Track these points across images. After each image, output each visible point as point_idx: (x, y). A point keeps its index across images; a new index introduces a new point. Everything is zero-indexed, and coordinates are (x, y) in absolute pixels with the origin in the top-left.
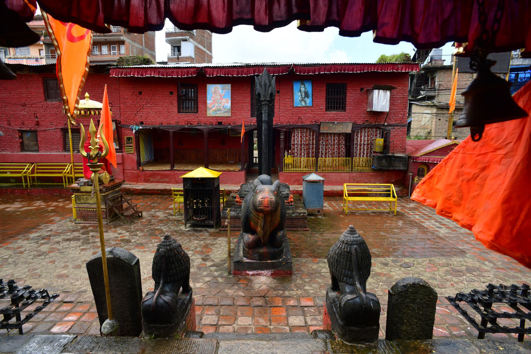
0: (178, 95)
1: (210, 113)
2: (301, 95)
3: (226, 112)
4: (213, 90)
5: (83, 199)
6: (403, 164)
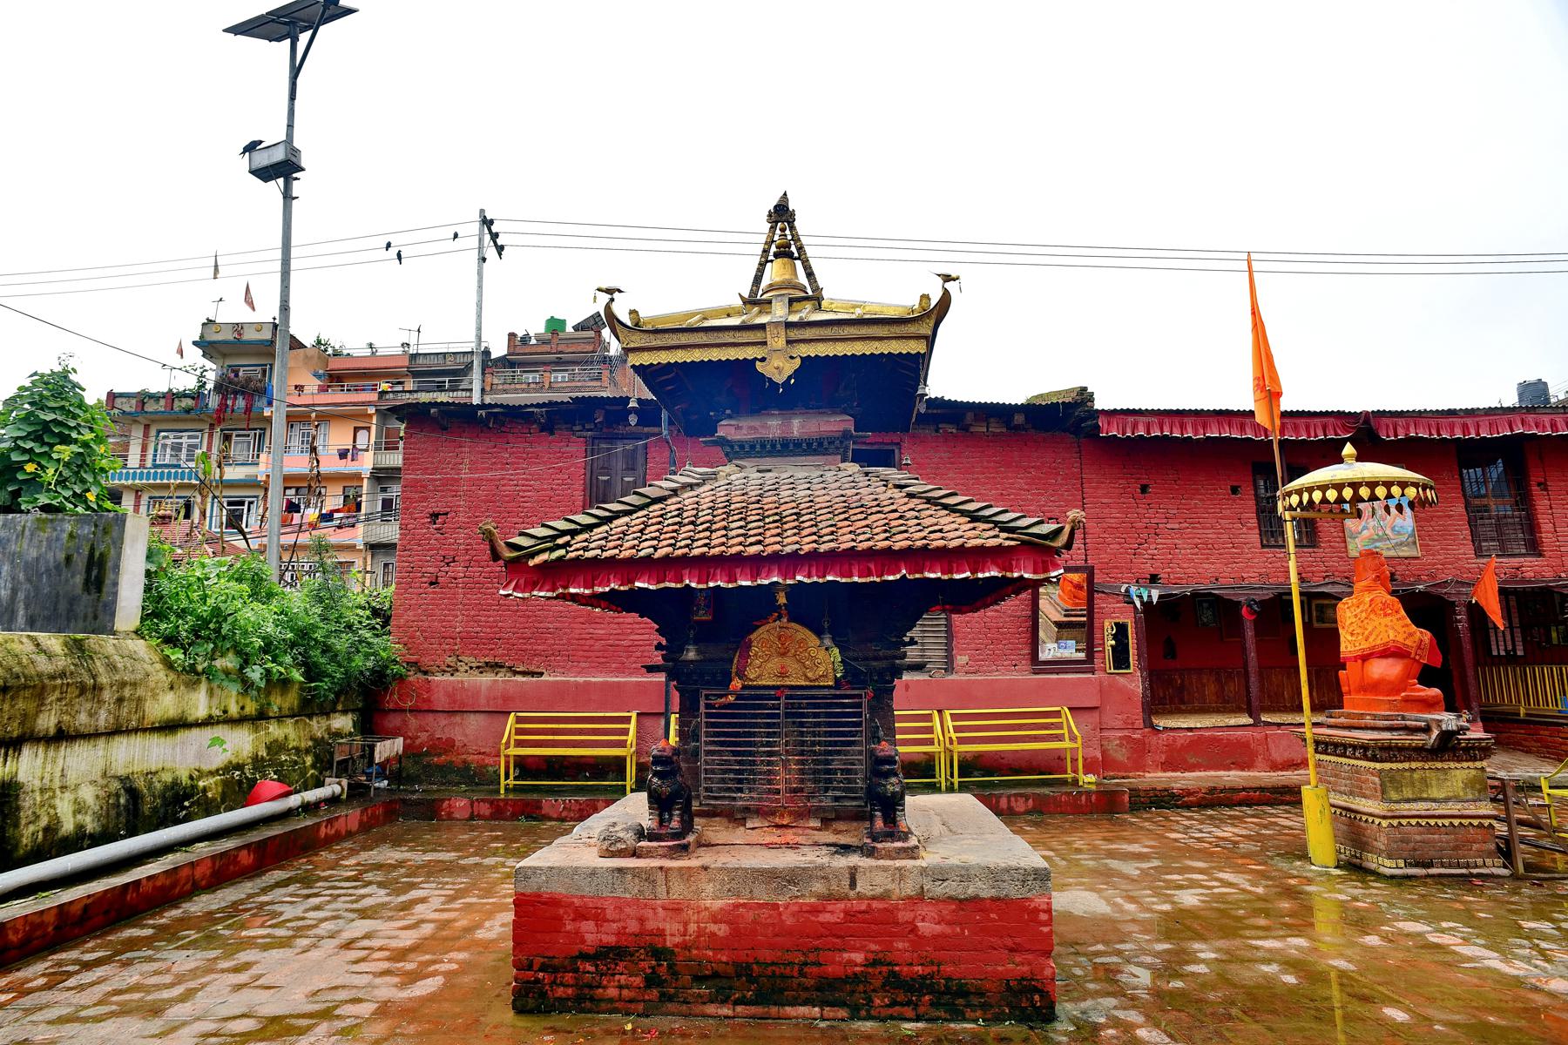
3: (1401, 544)
5: (1413, 784)
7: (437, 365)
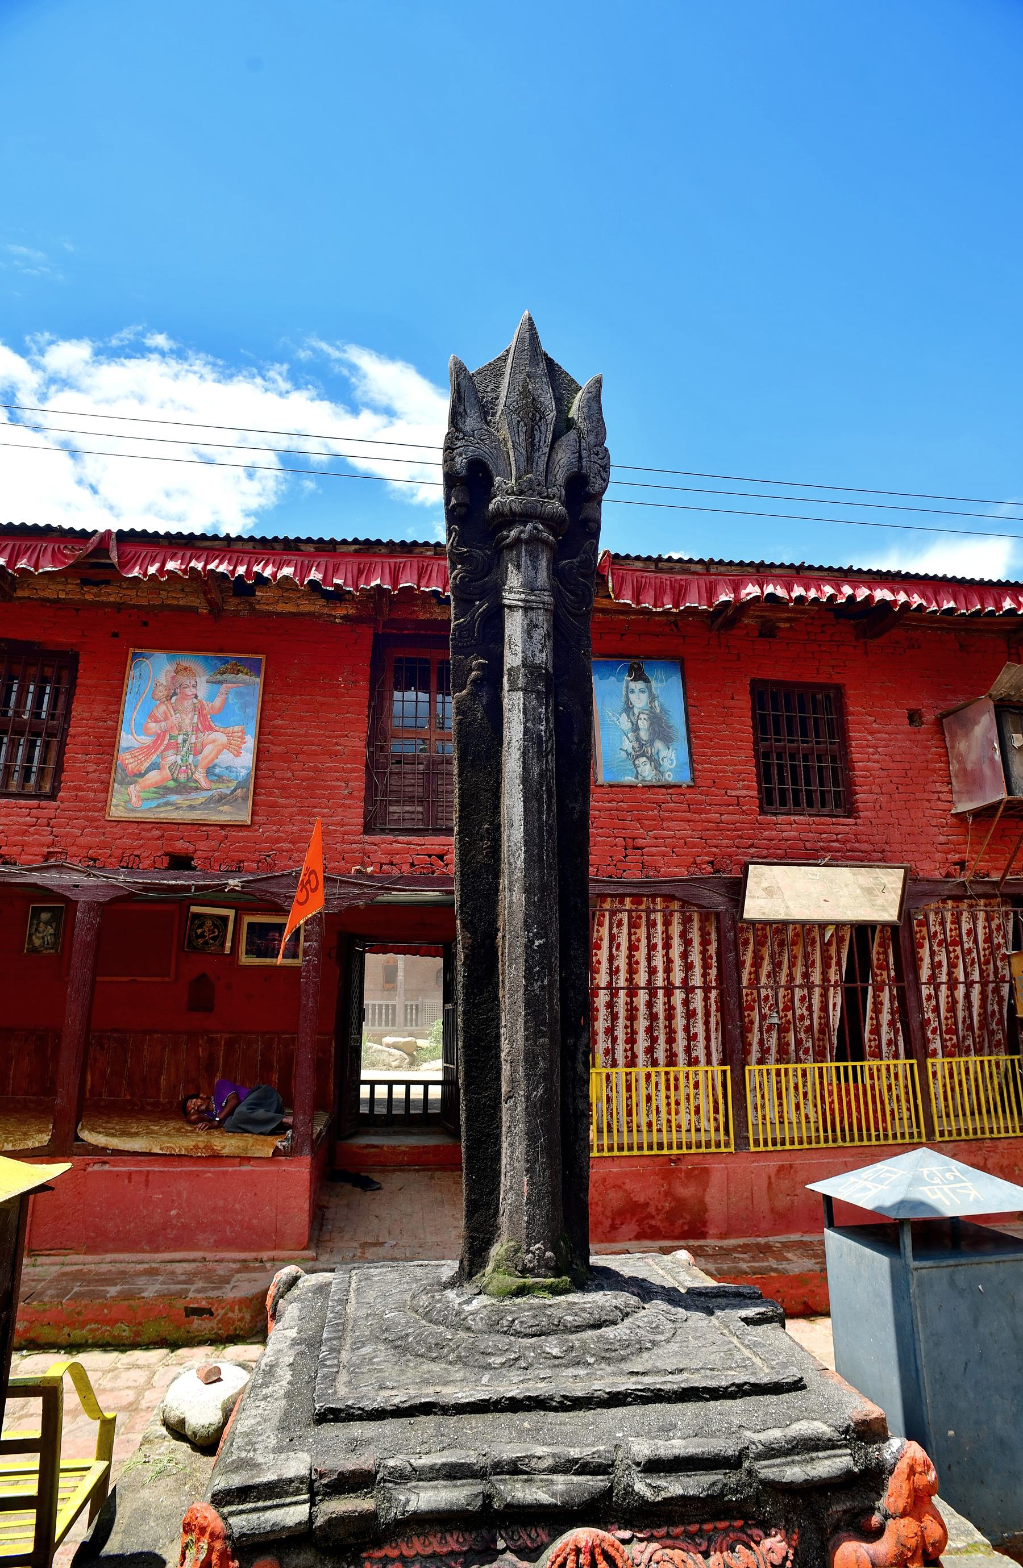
1: (130, 801)
3: (222, 799)
4: (163, 679)
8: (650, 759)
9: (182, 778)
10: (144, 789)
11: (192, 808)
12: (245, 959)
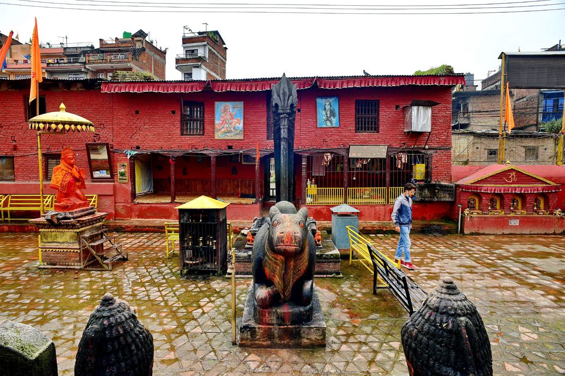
0: (181, 114)
1: (218, 136)
2: (327, 113)
3: (237, 134)
4: (222, 108)
5: (51, 237)
6: (449, 194)
7: (74, 52)
8: (330, 121)
9: (229, 130)
10: (221, 133)
11: (231, 136)
12: (244, 163)
